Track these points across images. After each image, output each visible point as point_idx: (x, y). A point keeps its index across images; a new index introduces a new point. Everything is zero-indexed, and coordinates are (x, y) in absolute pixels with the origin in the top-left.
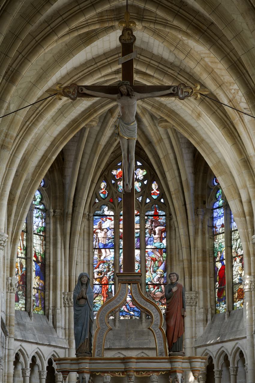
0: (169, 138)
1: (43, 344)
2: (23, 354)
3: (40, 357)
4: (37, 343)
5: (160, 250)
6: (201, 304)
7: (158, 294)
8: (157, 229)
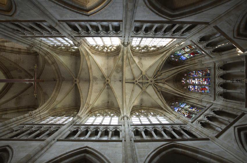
0: (166, 72)
1: (203, 113)
2: (201, 121)
3: (208, 115)
4: (201, 115)
5: (196, 72)
6: (201, 59)
7: (204, 73)
8: (192, 74)
